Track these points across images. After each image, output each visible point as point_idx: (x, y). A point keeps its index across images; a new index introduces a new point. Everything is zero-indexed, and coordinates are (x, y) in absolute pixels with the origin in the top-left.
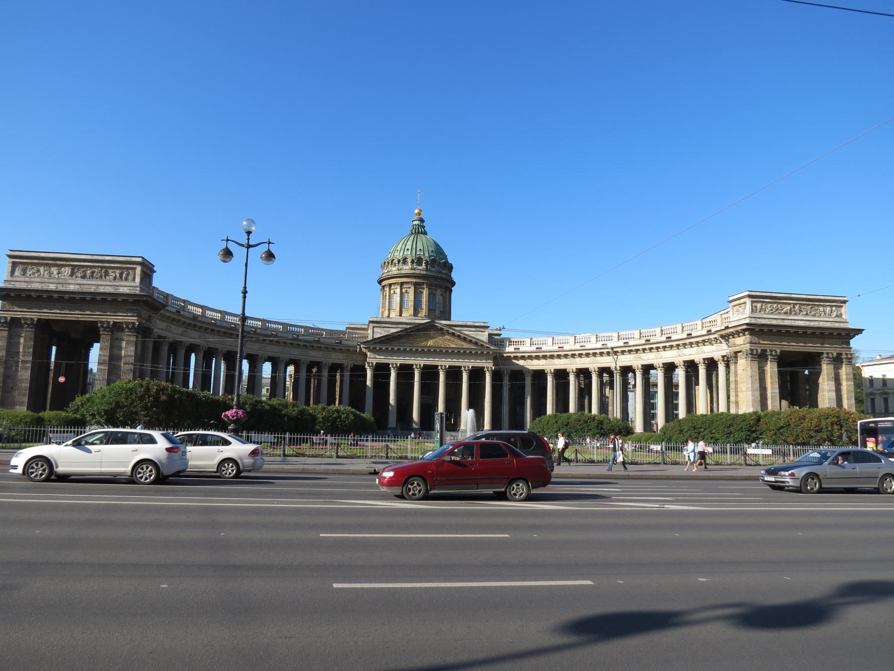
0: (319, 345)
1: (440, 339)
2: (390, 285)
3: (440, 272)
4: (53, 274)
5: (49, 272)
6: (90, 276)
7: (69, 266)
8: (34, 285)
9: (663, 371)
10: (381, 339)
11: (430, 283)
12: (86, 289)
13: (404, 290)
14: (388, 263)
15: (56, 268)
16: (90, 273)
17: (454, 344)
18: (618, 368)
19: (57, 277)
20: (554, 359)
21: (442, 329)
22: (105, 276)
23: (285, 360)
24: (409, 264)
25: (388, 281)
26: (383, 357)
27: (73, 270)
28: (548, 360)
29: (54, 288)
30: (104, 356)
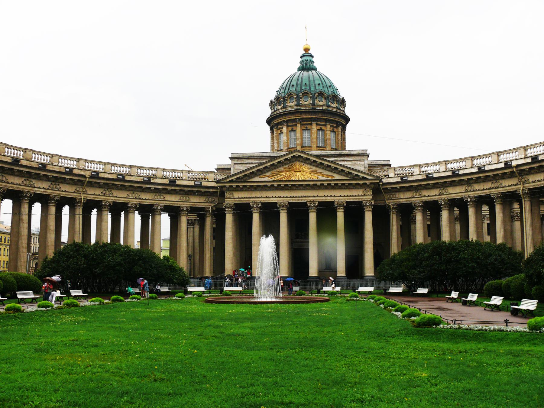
0: (173, 188)
2: (277, 125)
3: (329, 106)
10: (238, 176)
23: (134, 206)
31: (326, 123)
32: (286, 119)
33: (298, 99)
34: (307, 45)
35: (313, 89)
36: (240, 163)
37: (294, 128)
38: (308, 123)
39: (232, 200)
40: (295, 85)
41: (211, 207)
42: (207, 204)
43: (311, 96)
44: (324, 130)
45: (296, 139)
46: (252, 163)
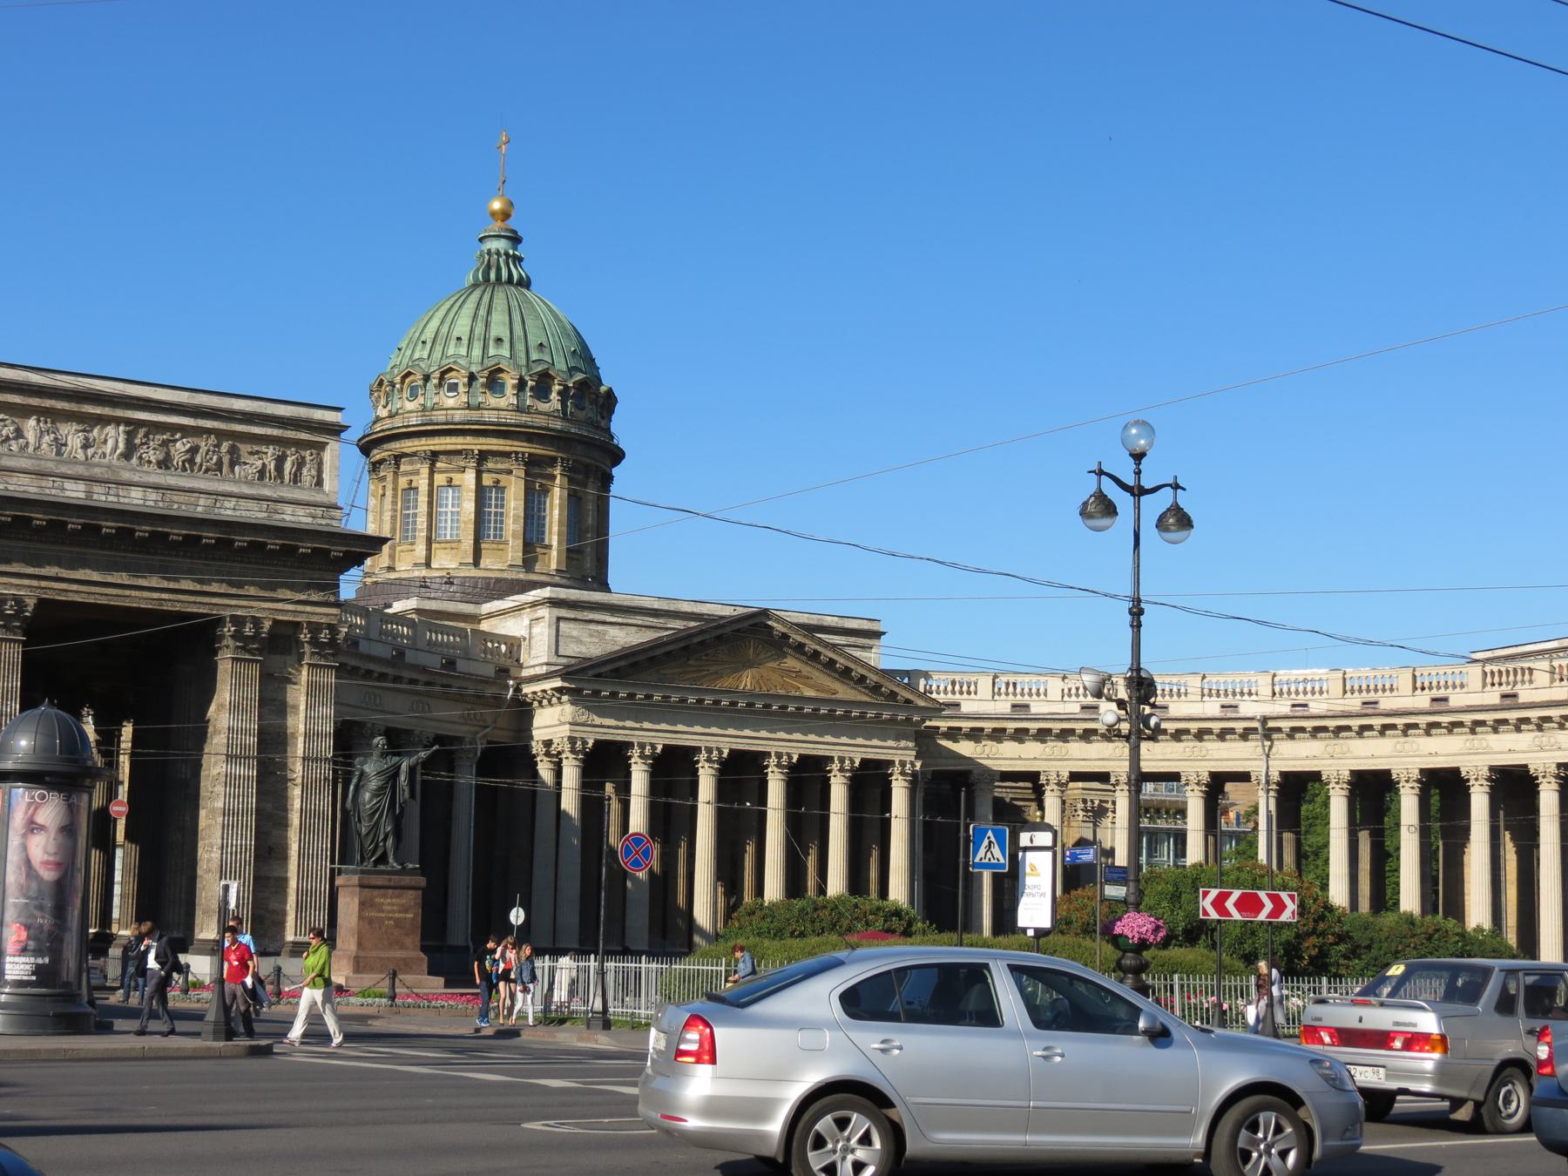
1: (773, 670)
2: (434, 456)
3: (598, 427)
4: (66, 445)
5: (56, 439)
6: (183, 462)
7: (118, 421)
8: (14, 480)
9: (1417, 791)
10: (617, 665)
11: (574, 461)
12: (180, 506)
13: (487, 480)
14: (427, 378)
15: (75, 426)
16: (187, 451)
17: (814, 685)
18: (1275, 777)
19: (80, 456)
20: (1068, 741)
21: (785, 636)
22: (232, 465)
24: (509, 391)
25: (423, 441)
26: (612, 722)
27: (130, 436)
28: (1049, 744)
29: (82, 495)
30: (246, 732)
32: (479, 447)
36: (573, 616)
40: (506, 340)
44: (580, 499)
46: (604, 623)
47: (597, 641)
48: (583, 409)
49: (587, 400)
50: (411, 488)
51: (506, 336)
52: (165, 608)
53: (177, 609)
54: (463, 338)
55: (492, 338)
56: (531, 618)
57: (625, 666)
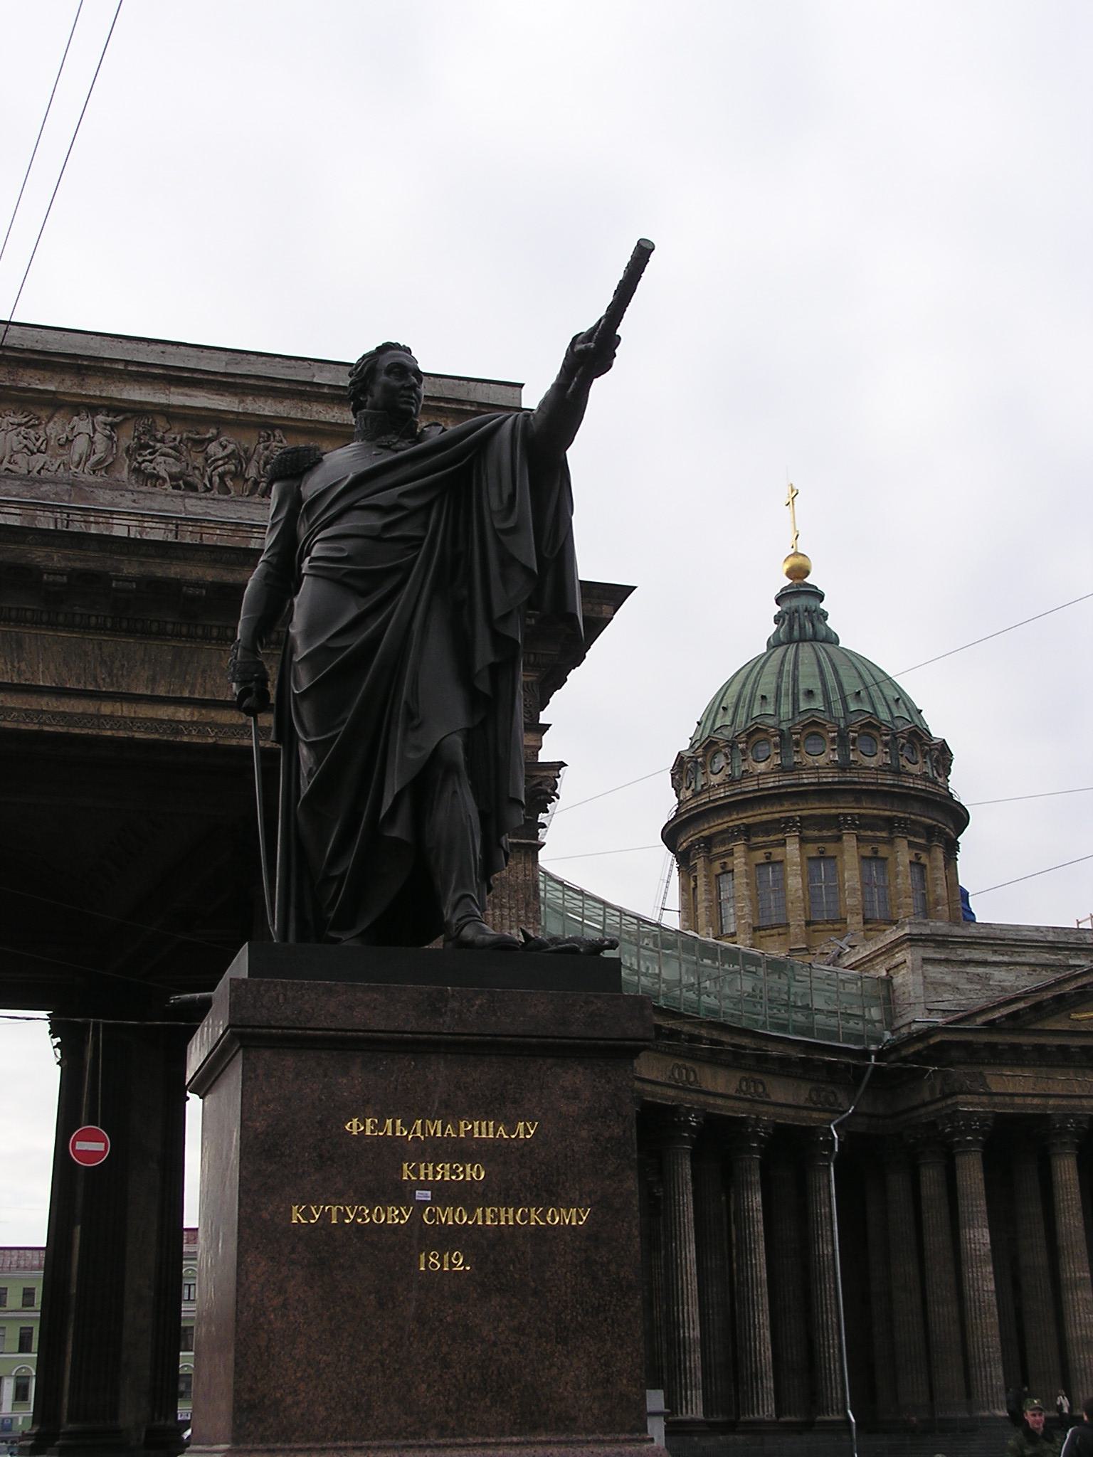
2: (747, 831)
3: (936, 783)
7: (91, 408)
10: (1014, 1008)
31: (929, 840)
32: (799, 813)
33: (843, 740)
34: (796, 554)
35: (884, 715)
36: (943, 957)
37: (831, 849)
38: (879, 834)
39: (985, 1099)
41: (834, 1126)
42: (815, 1115)
43: (887, 738)
44: (924, 866)
45: (841, 887)
46: (985, 963)
47: (979, 987)
48: (916, 763)
49: (919, 755)
50: (724, 873)
51: (817, 686)
52: (186, 739)
53: (210, 741)
54: (768, 696)
55: (801, 692)
56: (887, 966)
57: (1024, 1008)
